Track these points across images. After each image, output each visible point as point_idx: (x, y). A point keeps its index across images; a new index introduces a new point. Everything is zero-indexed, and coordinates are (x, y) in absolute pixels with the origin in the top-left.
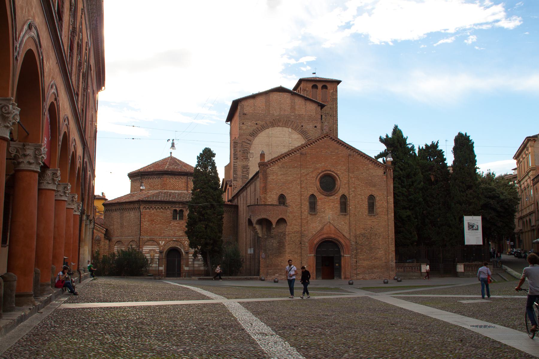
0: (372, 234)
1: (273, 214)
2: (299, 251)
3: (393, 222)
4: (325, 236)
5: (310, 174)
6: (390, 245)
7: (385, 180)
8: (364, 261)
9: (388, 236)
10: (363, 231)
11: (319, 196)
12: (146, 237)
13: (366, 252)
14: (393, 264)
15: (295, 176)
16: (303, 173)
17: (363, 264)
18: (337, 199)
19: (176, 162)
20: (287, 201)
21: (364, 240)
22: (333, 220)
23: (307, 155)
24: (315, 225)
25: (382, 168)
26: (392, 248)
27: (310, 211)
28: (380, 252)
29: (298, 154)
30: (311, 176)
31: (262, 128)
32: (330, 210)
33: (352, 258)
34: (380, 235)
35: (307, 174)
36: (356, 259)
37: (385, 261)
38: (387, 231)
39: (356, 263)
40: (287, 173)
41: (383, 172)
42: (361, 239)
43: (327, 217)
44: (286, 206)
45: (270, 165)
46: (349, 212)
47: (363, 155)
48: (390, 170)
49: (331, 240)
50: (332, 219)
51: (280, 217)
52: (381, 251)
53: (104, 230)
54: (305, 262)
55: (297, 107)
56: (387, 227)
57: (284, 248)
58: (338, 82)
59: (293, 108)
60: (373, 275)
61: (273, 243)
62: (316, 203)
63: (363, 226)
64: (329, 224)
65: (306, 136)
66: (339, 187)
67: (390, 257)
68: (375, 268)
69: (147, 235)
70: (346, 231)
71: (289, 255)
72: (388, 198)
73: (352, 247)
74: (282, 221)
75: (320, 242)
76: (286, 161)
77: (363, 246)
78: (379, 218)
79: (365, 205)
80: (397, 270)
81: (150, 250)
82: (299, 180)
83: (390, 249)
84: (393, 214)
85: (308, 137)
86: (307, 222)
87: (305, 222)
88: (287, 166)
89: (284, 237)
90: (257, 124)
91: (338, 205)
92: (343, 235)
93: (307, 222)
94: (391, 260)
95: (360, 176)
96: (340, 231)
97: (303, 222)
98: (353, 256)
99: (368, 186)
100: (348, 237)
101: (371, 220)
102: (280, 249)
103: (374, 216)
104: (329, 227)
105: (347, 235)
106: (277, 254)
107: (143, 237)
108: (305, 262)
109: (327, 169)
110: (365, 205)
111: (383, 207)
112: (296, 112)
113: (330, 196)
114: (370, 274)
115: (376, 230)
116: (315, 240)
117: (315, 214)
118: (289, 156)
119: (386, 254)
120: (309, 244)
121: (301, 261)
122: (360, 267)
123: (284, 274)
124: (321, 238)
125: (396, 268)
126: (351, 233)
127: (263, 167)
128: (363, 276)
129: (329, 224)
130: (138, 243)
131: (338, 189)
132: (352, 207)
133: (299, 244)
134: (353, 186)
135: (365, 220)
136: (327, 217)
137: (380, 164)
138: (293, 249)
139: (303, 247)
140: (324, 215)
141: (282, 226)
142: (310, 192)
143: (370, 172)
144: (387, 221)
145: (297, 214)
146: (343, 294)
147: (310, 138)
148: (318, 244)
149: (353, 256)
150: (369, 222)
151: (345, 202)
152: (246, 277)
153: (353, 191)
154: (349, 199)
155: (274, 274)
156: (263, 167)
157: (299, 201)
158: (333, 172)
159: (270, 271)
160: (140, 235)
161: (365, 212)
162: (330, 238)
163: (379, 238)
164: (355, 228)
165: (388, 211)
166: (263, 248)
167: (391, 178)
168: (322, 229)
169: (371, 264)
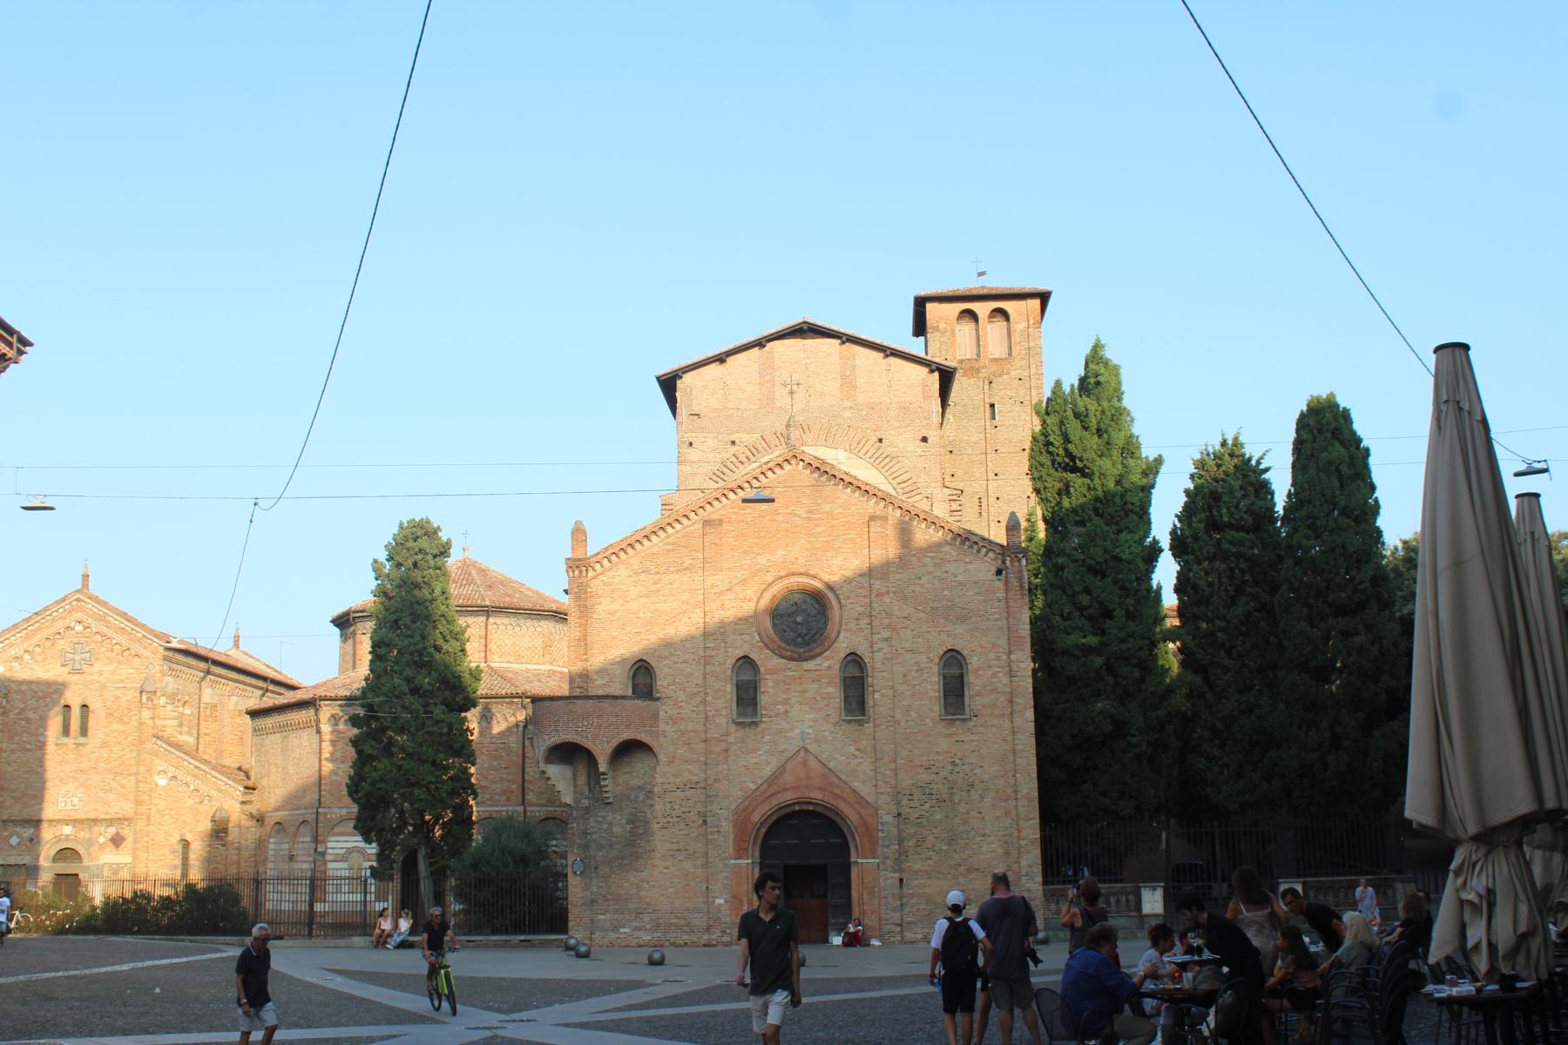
1: (599, 726)
3: (1033, 740)
4: (788, 797)
5: (738, 589)
6: (1021, 822)
7: (1001, 595)
8: (930, 878)
9: (1016, 791)
10: (925, 777)
11: (768, 662)
12: (336, 810)
13: (936, 849)
15: (685, 597)
16: (712, 586)
17: (927, 891)
18: (829, 668)
19: (470, 574)
20: (659, 683)
21: (927, 806)
22: (817, 741)
23: (725, 527)
25: (991, 555)
26: (1031, 829)
27: (740, 714)
28: (984, 848)
29: (694, 525)
30: (741, 596)
31: (749, 454)
32: (806, 708)
33: (886, 870)
35: (728, 590)
36: (900, 870)
38: (1010, 774)
39: (901, 886)
40: (658, 591)
41: (994, 570)
42: (916, 803)
43: (797, 731)
44: (658, 699)
45: (602, 566)
46: (872, 714)
47: (922, 516)
48: (1019, 561)
49: (811, 808)
50: (812, 736)
51: (625, 736)
52: (992, 843)
53: (240, 791)
54: (719, 885)
55: (860, 382)
56: (1011, 758)
57: (648, 841)
58: (1044, 297)
59: (848, 383)
61: (611, 824)
64: (802, 753)
65: (892, 471)
66: (836, 628)
67: (1024, 862)
69: (342, 805)
71: (666, 864)
72: (1013, 657)
73: (882, 830)
74: (628, 749)
75: (774, 818)
76: (655, 549)
78: (982, 730)
79: (932, 685)
80: (1053, 907)
81: (350, 851)
82: (698, 610)
83: (1024, 834)
84: (1030, 714)
85: (899, 473)
86: (726, 751)
87: (718, 748)
88: (657, 566)
89: (649, 802)
90: (733, 443)
91: (835, 692)
92: (854, 791)
93: (726, 751)
94: (1027, 875)
95: (912, 587)
96: (842, 777)
97: (712, 752)
98: (889, 862)
99: (942, 621)
101: (952, 735)
102: (634, 846)
103: (964, 720)
104: (805, 763)
105: (865, 790)
106: (625, 861)
107: (327, 810)
108: (719, 885)
109: (793, 569)
110: (929, 687)
111: (995, 690)
112: (861, 398)
113: (806, 660)
116: (752, 812)
117: (755, 724)
118: (666, 532)
119: (1007, 853)
120: (734, 826)
122: (913, 901)
123: (648, 927)
124: (775, 802)
125: (1047, 901)
126: (880, 783)
127: (577, 573)
129: (802, 753)
130: (314, 824)
131: (833, 635)
132: (882, 695)
133: (701, 826)
134: (886, 621)
136: (797, 731)
137: (981, 544)
140: (784, 725)
141: (640, 764)
142: (737, 648)
143: (947, 572)
144: (1010, 738)
145: (691, 726)
146: (631, 1007)
147: (905, 477)
148: (770, 822)
149: (889, 862)
150: (943, 744)
151: (863, 677)
152: (522, 938)
153: (886, 639)
154: (873, 668)
155: (616, 928)
156: (577, 573)
157: (700, 682)
159: (602, 917)
160: (320, 804)
161: (931, 710)
162: (810, 803)
163: (982, 797)
165: (1011, 702)
166: (578, 841)
167: (1022, 587)
168: (780, 771)
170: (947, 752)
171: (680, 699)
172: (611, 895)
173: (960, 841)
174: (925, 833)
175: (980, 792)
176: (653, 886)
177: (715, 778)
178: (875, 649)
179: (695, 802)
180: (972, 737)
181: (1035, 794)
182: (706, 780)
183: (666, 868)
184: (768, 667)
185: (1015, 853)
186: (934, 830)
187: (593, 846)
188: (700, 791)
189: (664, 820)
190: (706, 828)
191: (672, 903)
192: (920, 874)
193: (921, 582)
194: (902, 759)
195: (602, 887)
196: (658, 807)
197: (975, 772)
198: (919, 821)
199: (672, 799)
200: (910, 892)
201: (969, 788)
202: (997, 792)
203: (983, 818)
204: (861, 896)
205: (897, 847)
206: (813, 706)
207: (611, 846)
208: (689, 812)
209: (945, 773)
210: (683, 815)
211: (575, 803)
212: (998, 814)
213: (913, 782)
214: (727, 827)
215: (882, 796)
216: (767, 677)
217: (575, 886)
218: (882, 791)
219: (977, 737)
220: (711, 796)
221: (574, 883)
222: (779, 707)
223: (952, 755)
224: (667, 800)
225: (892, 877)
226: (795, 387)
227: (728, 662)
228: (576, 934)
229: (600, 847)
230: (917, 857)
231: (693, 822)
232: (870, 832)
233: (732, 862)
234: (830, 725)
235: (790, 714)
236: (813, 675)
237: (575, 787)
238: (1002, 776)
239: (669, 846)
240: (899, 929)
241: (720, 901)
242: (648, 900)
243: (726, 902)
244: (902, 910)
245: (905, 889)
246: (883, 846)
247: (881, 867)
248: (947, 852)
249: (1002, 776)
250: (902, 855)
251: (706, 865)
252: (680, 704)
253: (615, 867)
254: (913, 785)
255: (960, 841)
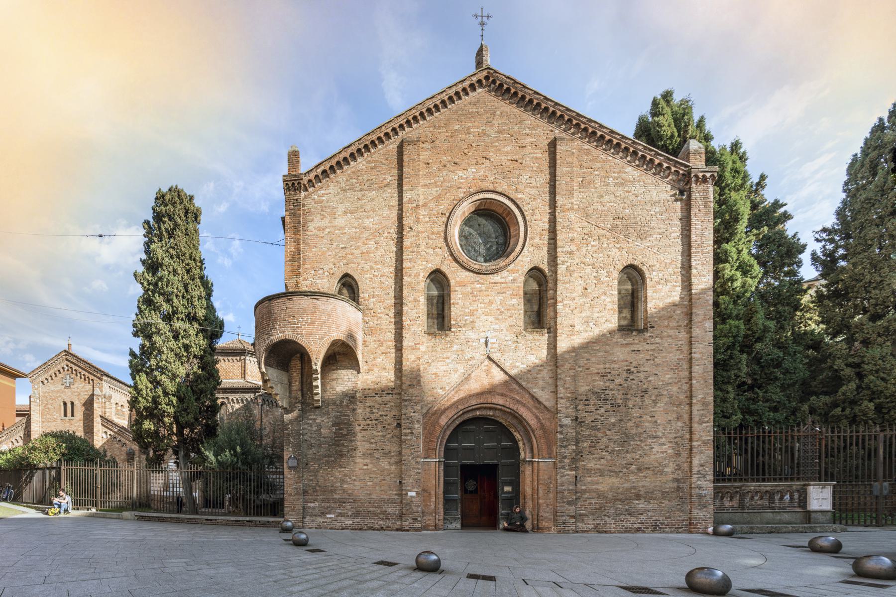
0: (632, 392)
2: (394, 448)
10: (602, 384)
13: (610, 449)
14: (705, 485)
18: (514, 281)
20: (361, 295)
21: (603, 410)
24: (444, 368)
28: (656, 449)
32: (491, 319)
33: (563, 467)
34: (660, 395)
36: (576, 469)
37: (675, 476)
54: (411, 481)
57: (351, 441)
60: (633, 520)
61: (320, 426)
62: (446, 298)
63: (602, 366)
68: (638, 497)
70: (541, 383)
71: (366, 461)
73: (561, 433)
77: (598, 430)
91: (517, 304)
98: (567, 461)
100: (547, 404)
105: (544, 396)
108: (411, 481)
114: (622, 517)
115: (646, 378)
120: (425, 429)
121: (401, 476)
126: (561, 389)
128: (598, 522)
129: (487, 362)
135: (608, 348)
138: (376, 443)
139: (406, 435)
149: (567, 461)
152: (248, 519)
158: (501, 194)
159: (312, 505)
163: (655, 402)
164: (572, 373)
168: (467, 378)
169: (627, 485)
170: (622, 361)
171: (379, 311)
172: (319, 486)
173: (632, 443)
174: (599, 435)
175: (653, 398)
176: (355, 480)
177: (409, 383)
178: (559, 262)
179: (392, 406)
180: (647, 347)
181: (711, 399)
182: (401, 386)
183: (365, 465)
184: (458, 279)
185: (685, 454)
186: (608, 433)
187: (305, 445)
188: (395, 396)
189: (364, 423)
190: (401, 430)
191: (370, 494)
192: (593, 472)
193: (602, 200)
194: (579, 367)
195: (312, 480)
196: (359, 411)
197: (650, 379)
198: (593, 424)
199: (372, 404)
200: (583, 488)
201: (643, 394)
202: (670, 398)
203: (656, 422)
204: (535, 491)
205: (574, 447)
206: (500, 317)
207: (320, 446)
208: (386, 416)
209: (620, 380)
210: (381, 418)
211: (290, 406)
212: (670, 418)
213: (588, 388)
214: (418, 428)
215: (562, 401)
216: (457, 289)
217: (290, 479)
218: (562, 395)
219: (652, 347)
220: (406, 400)
221: (289, 476)
222: (466, 318)
223: (627, 363)
224: (368, 404)
225: (568, 475)
226: (485, 19)
227: (422, 274)
228: (291, 520)
229: (311, 446)
230: (591, 457)
231: (389, 425)
232: (549, 436)
233: (422, 460)
234: (514, 335)
235: (477, 325)
236: (498, 287)
237: (290, 393)
238: (675, 383)
239: (367, 446)
240: (574, 520)
241: (414, 494)
242: (350, 492)
243: (417, 493)
244: (576, 504)
245: (578, 485)
246: (561, 446)
247: (559, 465)
248: (619, 452)
249: (675, 383)
250: (578, 456)
251: (400, 462)
252: (379, 315)
253: (323, 463)
254: (589, 391)
255: (632, 443)
